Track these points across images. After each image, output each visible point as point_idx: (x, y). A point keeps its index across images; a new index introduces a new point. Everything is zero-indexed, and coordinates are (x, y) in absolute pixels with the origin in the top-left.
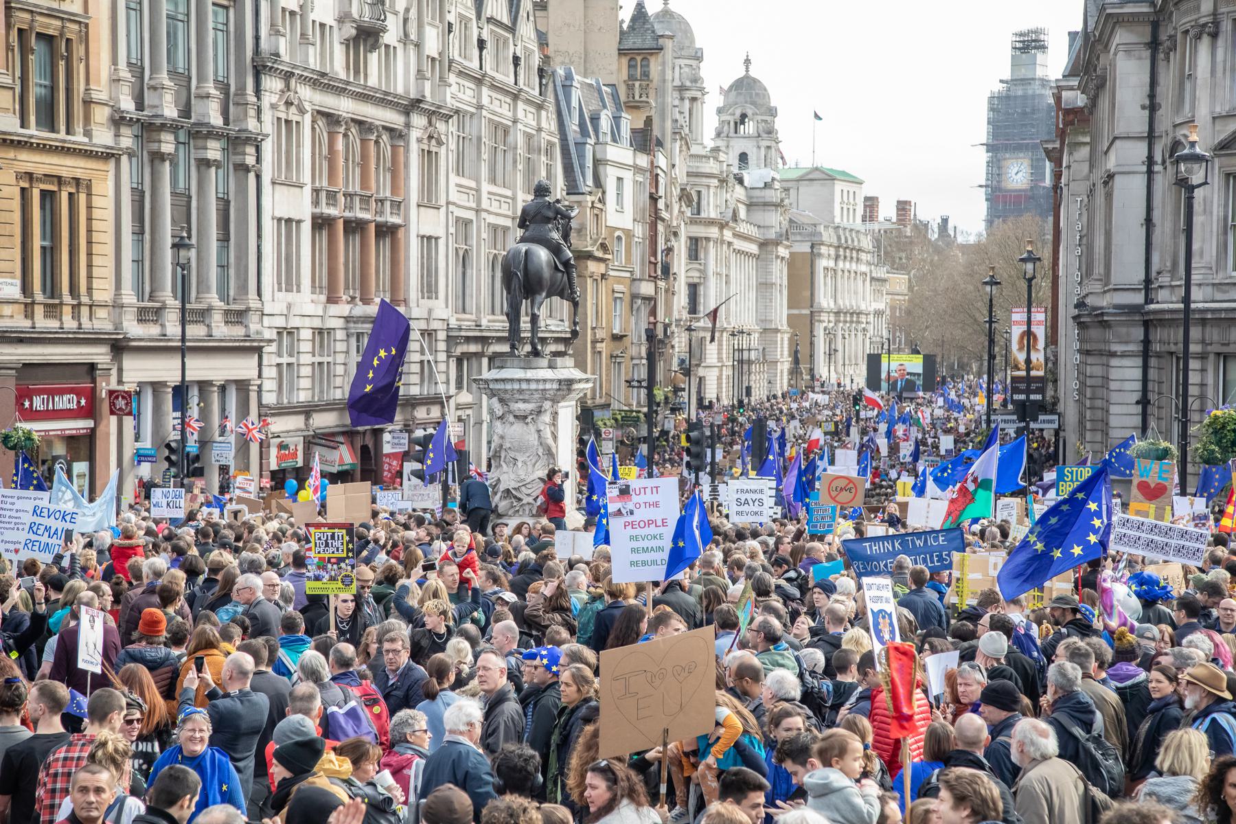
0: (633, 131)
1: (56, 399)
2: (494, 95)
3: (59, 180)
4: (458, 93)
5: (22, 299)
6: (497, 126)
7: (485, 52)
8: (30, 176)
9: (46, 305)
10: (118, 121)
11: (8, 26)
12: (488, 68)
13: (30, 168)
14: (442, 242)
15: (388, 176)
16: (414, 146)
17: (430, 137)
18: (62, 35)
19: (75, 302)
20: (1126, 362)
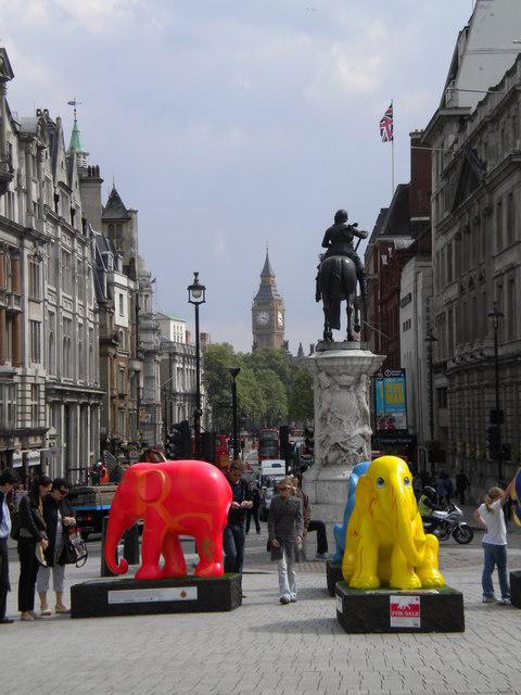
0: (124, 267)
4: (47, 229)
12: (60, 214)
14: (41, 325)
15: (10, 279)
16: (26, 260)
17: (36, 255)
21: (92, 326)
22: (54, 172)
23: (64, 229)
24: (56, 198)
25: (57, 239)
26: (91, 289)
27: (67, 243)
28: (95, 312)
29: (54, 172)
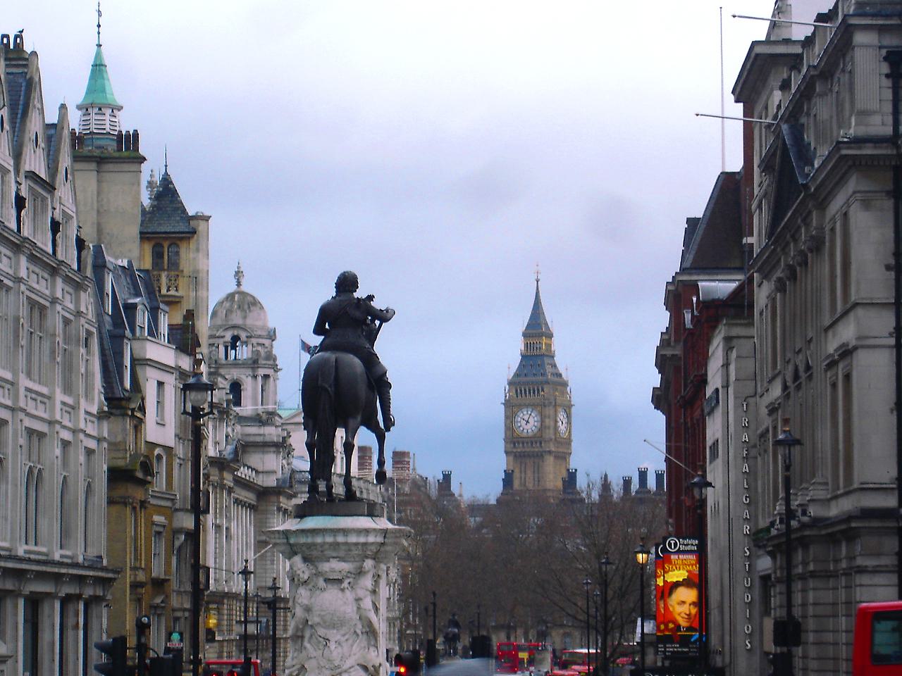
0: (171, 327)
2: (32, 267)
6: (33, 304)
7: (23, 212)
12: (26, 232)
20: (879, 579)
21: (92, 444)
22: (17, 155)
23: (33, 258)
24: (20, 203)
25: (19, 280)
26: (88, 375)
27: (42, 287)
28: (101, 416)
29: (17, 155)
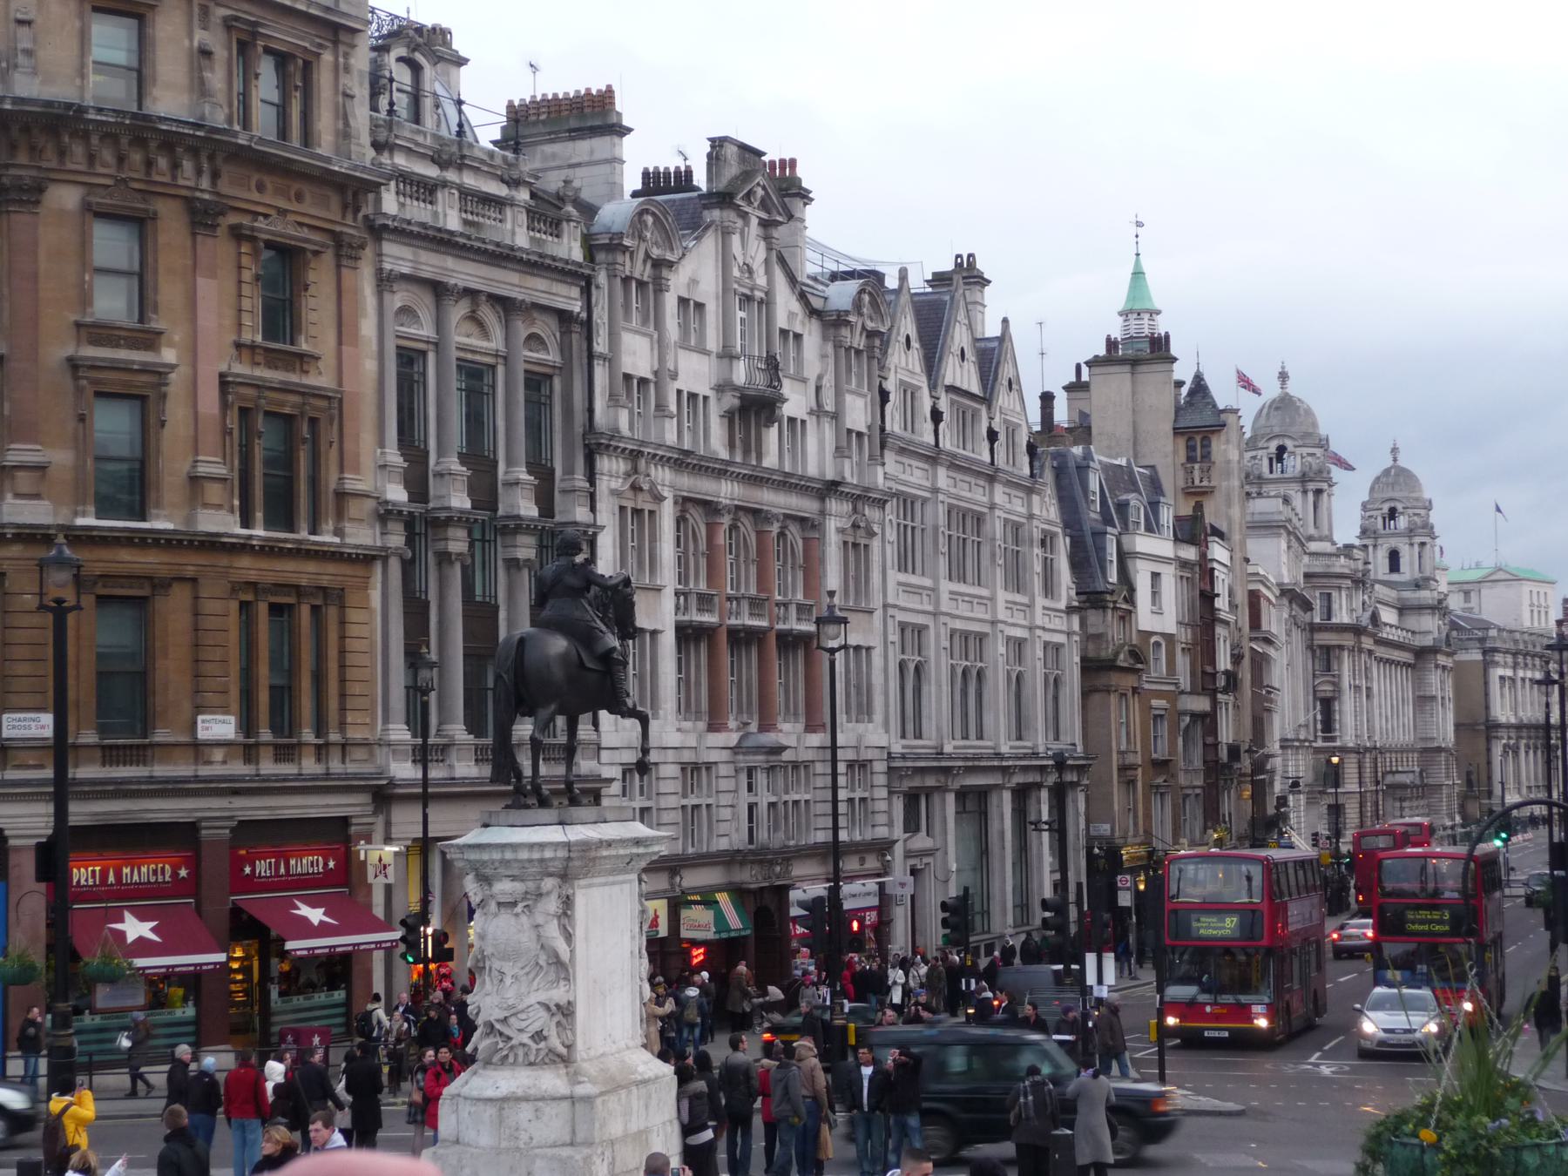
1: (293, 862)
3: (297, 590)
5: (241, 739)
8: (253, 586)
9: (276, 746)
10: (386, 515)
11: (225, 406)
13: (253, 576)
18: (302, 414)
19: (321, 741)
